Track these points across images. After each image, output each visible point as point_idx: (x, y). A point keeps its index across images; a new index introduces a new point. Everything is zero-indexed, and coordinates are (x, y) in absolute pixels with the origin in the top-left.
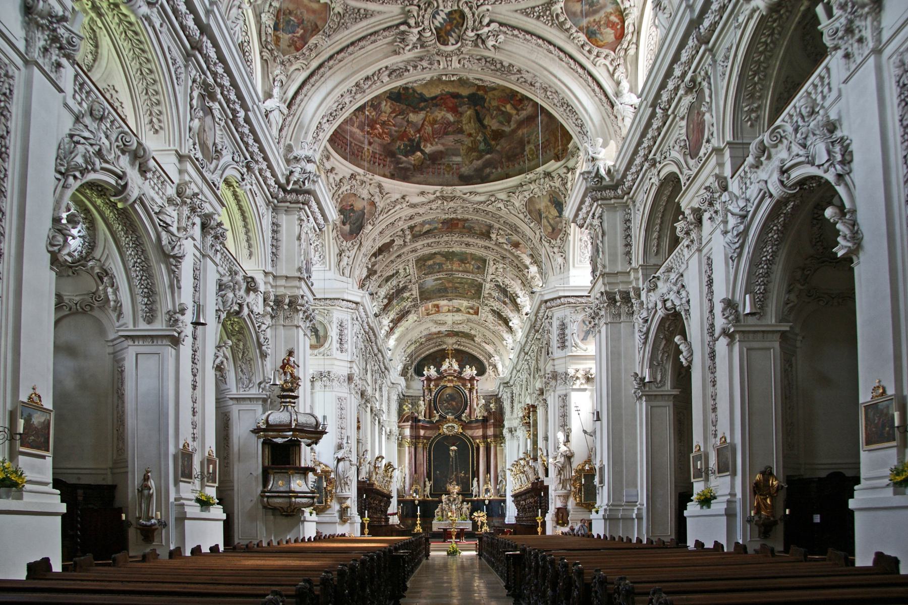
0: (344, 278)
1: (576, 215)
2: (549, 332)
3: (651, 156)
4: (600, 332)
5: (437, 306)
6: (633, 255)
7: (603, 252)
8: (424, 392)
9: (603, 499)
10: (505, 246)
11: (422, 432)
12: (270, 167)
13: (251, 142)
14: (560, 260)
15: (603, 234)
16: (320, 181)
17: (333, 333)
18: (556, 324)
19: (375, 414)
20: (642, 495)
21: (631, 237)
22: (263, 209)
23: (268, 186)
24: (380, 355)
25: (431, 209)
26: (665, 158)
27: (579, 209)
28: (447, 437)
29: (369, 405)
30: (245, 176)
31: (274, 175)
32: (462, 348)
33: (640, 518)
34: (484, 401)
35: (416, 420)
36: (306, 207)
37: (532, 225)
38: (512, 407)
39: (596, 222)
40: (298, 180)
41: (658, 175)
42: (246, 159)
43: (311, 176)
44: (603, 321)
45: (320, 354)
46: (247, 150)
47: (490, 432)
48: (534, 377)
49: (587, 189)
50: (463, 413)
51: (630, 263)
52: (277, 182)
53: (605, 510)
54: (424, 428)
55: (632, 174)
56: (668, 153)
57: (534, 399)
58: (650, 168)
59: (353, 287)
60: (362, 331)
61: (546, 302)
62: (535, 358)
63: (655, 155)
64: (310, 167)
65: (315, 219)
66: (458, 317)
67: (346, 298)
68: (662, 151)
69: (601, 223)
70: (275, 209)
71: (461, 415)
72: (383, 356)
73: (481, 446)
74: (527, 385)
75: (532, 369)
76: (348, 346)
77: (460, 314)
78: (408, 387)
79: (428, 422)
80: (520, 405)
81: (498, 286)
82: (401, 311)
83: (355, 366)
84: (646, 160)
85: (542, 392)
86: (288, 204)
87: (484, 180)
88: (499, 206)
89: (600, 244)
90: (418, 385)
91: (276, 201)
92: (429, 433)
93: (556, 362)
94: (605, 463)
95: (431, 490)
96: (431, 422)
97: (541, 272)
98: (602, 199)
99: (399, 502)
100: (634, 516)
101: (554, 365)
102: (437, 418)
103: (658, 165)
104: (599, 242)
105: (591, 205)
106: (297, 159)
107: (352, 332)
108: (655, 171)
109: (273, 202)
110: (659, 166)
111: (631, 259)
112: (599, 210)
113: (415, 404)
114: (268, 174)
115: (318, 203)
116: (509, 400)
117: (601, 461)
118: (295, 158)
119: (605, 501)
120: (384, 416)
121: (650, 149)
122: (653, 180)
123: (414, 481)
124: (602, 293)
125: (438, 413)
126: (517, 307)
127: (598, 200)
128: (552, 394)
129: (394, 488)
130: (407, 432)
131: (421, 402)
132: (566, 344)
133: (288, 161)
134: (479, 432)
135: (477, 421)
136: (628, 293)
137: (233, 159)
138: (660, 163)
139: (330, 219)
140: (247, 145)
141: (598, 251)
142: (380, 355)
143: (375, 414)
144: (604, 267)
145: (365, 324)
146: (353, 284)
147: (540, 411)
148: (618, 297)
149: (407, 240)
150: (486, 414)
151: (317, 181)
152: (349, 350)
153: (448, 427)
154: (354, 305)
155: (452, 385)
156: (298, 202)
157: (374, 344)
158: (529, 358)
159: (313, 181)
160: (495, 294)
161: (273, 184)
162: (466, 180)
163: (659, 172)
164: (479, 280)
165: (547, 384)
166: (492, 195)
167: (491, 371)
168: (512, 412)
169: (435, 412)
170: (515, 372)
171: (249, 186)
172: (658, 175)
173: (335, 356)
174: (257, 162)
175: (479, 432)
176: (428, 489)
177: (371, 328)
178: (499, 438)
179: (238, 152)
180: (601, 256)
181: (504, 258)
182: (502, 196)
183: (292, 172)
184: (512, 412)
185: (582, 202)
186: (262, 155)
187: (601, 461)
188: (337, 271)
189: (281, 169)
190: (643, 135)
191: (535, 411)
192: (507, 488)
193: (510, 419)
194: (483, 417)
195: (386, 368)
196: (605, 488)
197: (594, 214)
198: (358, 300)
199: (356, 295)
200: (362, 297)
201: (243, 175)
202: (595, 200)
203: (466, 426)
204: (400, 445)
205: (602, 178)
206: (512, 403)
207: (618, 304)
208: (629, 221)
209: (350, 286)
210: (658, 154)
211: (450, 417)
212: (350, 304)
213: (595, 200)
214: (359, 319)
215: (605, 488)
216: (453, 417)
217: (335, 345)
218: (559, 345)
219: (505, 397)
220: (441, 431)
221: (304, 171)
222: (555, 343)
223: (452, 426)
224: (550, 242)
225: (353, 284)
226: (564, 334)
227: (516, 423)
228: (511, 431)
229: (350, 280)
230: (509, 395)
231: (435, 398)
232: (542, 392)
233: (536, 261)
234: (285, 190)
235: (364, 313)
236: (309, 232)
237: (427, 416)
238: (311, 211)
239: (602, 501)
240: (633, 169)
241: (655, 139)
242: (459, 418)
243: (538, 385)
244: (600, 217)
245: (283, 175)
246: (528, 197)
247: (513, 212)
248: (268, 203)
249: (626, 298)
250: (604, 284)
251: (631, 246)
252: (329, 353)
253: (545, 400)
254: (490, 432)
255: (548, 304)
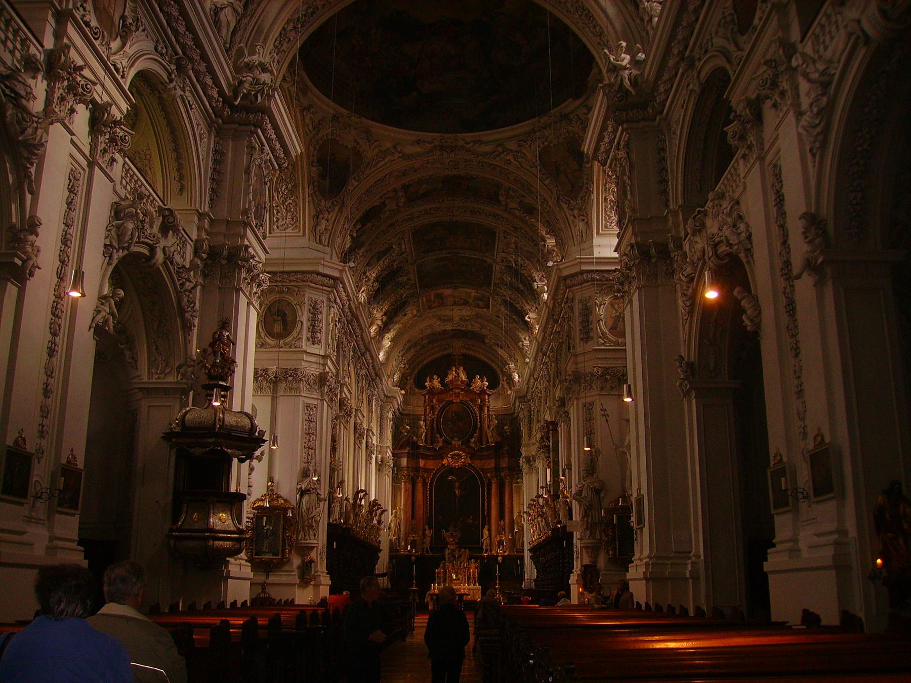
0: (320, 247)
1: (597, 148)
2: (570, 319)
3: (687, 53)
4: (631, 302)
5: (439, 296)
6: (671, 194)
7: (631, 190)
8: (425, 410)
9: (643, 548)
10: (517, 213)
11: (422, 463)
12: (211, 70)
13: (182, 29)
14: (581, 225)
15: (632, 167)
16: (276, 95)
17: (304, 317)
18: (577, 307)
19: (359, 433)
20: (697, 541)
21: (667, 171)
22: (201, 127)
23: (210, 98)
24: (368, 355)
25: (428, 163)
26: (706, 51)
27: (600, 138)
28: (451, 470)
29: (352, 420)
30: (173, 76)
31: (217, 83)
32: (472, 353)
33: (695, 577)
34: (496, 422)
35: (414, 446)
36: (259, 131)
37: (547, 182)
38: (530, 429)
39: (622, 154)
40: (249, 93)
41: (698, 76)
42: (177, 54)
43: (266, 89)
44: (635, 284)
45: (285, 345)
46: (177, 40)
47: (504, 463)
48: (554, 387)
49: (608, 107)
50: (472, 437)
51: (667, 206)
52: (221, 93)
53: (647, 564)
54: (425, 457)
55: (664, 83)
56: (710, 44)
57: (553, 412)
58: (687, 71)
59: (331, 258)
60: (343, 319)
61: (565, 278)
62: (554, 359)
63: (692, 51)
64: (265, 77)
65: (273, 150)
66: (466, 312)
67: (321, 270)
68: (701, 44)
69: (628, 153)
70: (219, 133)
71: (469, 441)
72: (372, 357)
73: (493, 481)
74: (546, 396)
75: (552, 375)
76: (322, 336)
77: (468, 308)
78: (406, 402)
79: (429, 449)
80: (539, 425)
81: (510, 267)
82: (396, 301)
83: (329, 363)
84: (682, 59)
85: (563, 403)
86: (236, 126)
87: (491, 125)
88: (508, 158)
89: (628, 181)
90: (418, 406)
91: (220, 121)
92: (431, 464)
93: (580, 359)
94: (644, 491)
95: (431, 542)
96: (434, 448)
97: (561, 244)
98: (627, 121)
99: (391, 558)
100: (688, 576)
101: (577, 364)
102: (440, 444)
103: (697, 63)
104: (626, 178)
105: (615, 131)
106: (249, 67)
107: (329, 316)
108: (695, 73)
109: (218, 124)
110: (699, 65)
111: (668, 200)
112: (625, 137)
113: (415, 426)
114: (209, 81)
115: (276, 127)
116: (526, 420)
117: (639, 489)
118: (247, 65)
119: (646, 552)
120: (374, 438)
121: (686, 40)
122: (691, 86)
123: (412, 528)
124: (632, 246)
125: (441, 437)
126: (535, 295)
127: (623, 122)
128: (575, 403)
129: (385, 538)
130: (404, 462)
131: (422, 423)
132: (591, 334)
133: (237, 69)
134: (491, 464)
135: (488, 447)
136: (666, 245)
137: (156, 50)
138: (699, 60)
139: (293, 154)
140: (176, 32)
141: (625, 193)
142: (368, 355)
143: (359, 433)
144: (633, 210)
145: (347, 310)
146: (331, 255)
147: (561, 430)
148: (653, 251)
149: (401, 204)
150: (499, 439)
151: (274, 95)
152: (323, 341)
153: (455, 455)
154: (332, 282)
155: (458, 401)
156: (249, 124)
157: (359, 339)
158: (547, 360)
159: (268, 94)
160: (508, 279)
161: (216, 96)
162: (469, 127)
163: (699, 72)
164: (488, 260)
165: (568, 389)
166: (500, 145)
167: (505, 383)
168: (530, 435)
169: (438, 435)
170: (532, 380)
171: (179, 92)
172: (698, 76)
173: (304, 348)
174: (191, 60)
175: (491, 464)
176: (428, 539)
177: (354, 316)
178: (515, 472)
179: (164, 42)
180: (629, 197)
181: (516, 228)
182: (512, 146)
183: (241, 83)
184: (530, 435)
185: (604, 128)
186: (191, 36)
187: (639, 489)
188: (312, 238)
189: (225, 72)
190: (676, 24)
191: (555, 431)
192: (525, 539)
193: (528, 445)
194: (496, 443)
195: (376, 375)
196: (646, 530)
197: (619, 143)
198: (336, 274)
199: (331, 267)
200: (341, 271)
201: (170, 74)
202: (618, 123)
203: (473, 455)
204: (395, 480)
205: (627, 92)
206: (530, 424)
207: (653, 260)
208: (663, 149)
209: (327, 257)
210: (697, 49)
211: (456, 442)
212: (326, 281)
213: (618, 123)
214: (338, 301)
215: (646, 530)
216: (460, 443)
217: (305, 334)
218: (582, 336)
219: (521, 415)
220: (445, 462)
221: (256, 82)
222: (577, 335)
223: (458, 455)
224: (570, 203)
225: (331, 255)
226: (588, 321)
227: (534, 450)
228: (528, 461)
229: (328, 249)
230: (526, 413)
231: (439, 417)
232: (563, 403)
233: (553, 232)
234: (234, 108)
235: (343, 293)
236: (263, 165)
237: (429, 442)
238: (266, 138)
239: (642, 552)
240: (666, 76)
241: (691, 26)
242: (466, 443)
243: (558, 394)
244: (627, 146)
245: (229, 84)
246: (542, 146)
247: (524, 165)
248: (210, 124)
249: (664, 253)
250: (634, 233)
251: (667, 182)
252: (297, 343)
253: (567, 413)
254: (504, 463)
255: (568, 282)
